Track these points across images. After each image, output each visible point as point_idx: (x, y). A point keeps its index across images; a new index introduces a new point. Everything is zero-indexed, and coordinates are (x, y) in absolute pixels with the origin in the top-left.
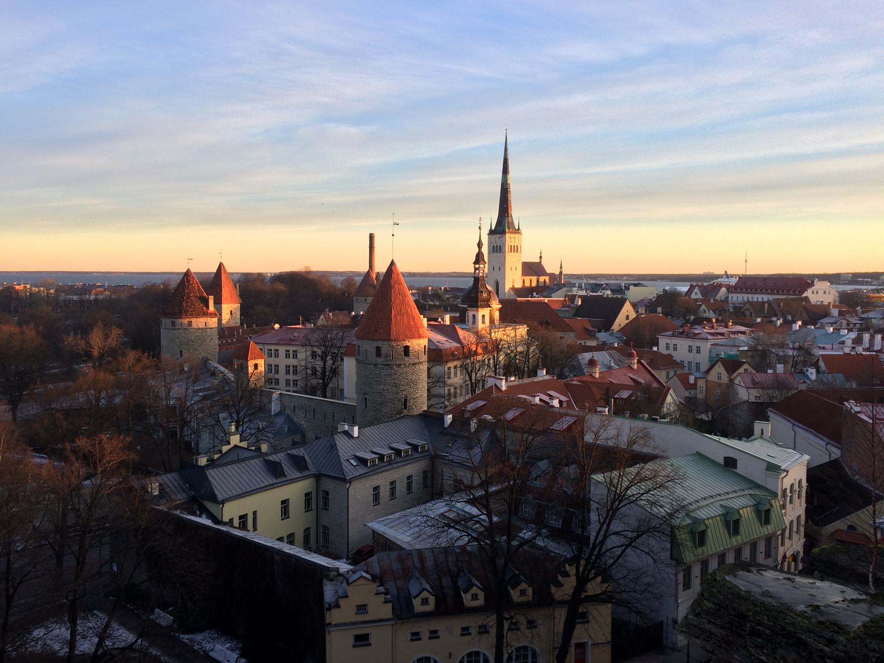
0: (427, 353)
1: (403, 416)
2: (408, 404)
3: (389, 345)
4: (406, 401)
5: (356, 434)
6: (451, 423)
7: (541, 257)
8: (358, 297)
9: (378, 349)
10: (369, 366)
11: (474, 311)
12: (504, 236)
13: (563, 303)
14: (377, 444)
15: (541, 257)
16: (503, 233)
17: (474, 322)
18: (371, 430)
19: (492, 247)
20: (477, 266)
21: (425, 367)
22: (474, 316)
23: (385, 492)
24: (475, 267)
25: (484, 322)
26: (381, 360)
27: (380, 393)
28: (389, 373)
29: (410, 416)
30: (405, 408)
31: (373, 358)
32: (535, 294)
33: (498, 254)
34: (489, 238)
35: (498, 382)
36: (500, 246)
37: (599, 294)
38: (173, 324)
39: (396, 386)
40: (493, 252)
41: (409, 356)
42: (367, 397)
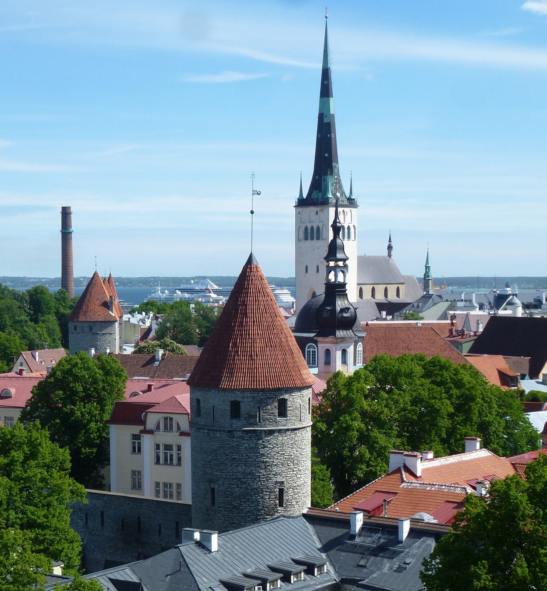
0: (311, 411)
1: (278, 517)
2: (285, 498)
3: (254, 398)
4: (281, 491)
5: (214, 547)
6: (362, 529)
7: (390, 248)
8: (76, 324)
9: (235, 407)
10: (218, 435)
11: (326, 342)
12: (325, 210)
13: (451, 331)
14: (249, 562)
15: (390, 248)
16: (325, 203)
18: (240, 535)
19: (303, 227)
20: (332, 264)
21: (307, 435)
22: (328, 352)
24: (328, 266)
26: (239, 424)
27: (239, 479)
28: (252, 445)
29: (289, 517)
30: (281, 505)
31: (226, 421)
32: (384, 313)
33: (315, 243)
34: (298, 214)
35: (409, 461)
36: (318, 227)
37: (501, 312)
39: (265, 467)
40: (306, 239)
41: (285, 417)
42: (216, 486)
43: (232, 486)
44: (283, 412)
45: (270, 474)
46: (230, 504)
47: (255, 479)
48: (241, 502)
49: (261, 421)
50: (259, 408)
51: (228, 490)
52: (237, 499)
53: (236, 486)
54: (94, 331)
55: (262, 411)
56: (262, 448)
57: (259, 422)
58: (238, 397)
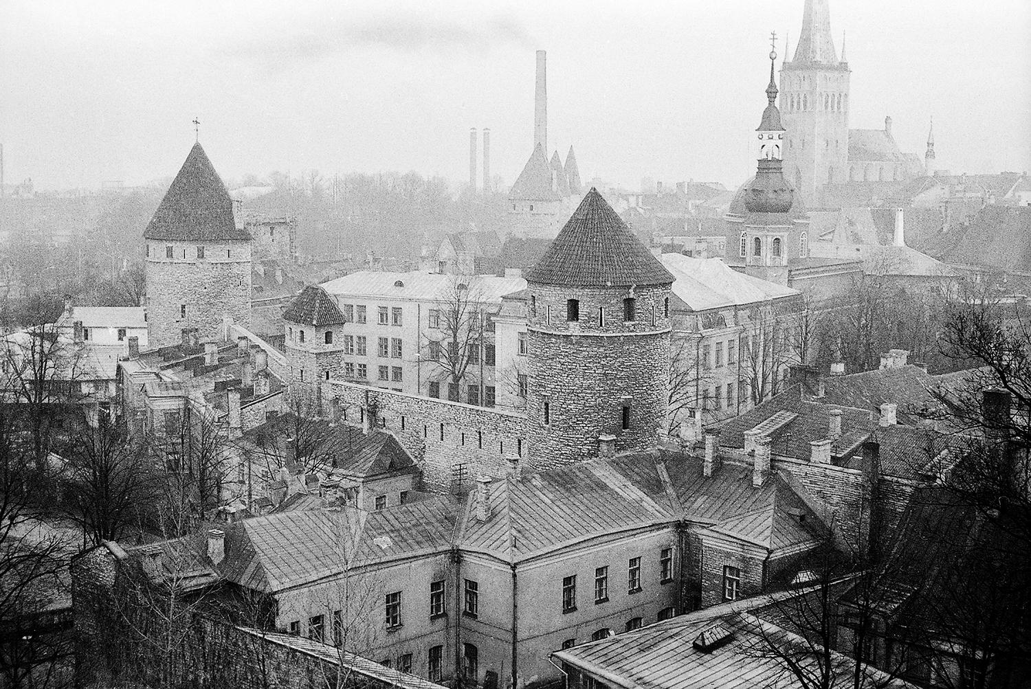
4: (626, 410)
9: (573, 306)
17: (758, 252)
23: (585, 590)
25: (777, 252)
38: (170, 253)
43: (567, 402)
44: (629, 316)
45: (613, 389)
46: (565, 423)
47: (595, 394)
48: (578, 421)
49: (603, 325)
50: (601, 309)
51: (563, 406)
52: (573, 417)
53: (572, 402)
54: (535, 211)
55: (603, 312)
56: (603, 357)
57: (601, 325)
58: (575, 294)
